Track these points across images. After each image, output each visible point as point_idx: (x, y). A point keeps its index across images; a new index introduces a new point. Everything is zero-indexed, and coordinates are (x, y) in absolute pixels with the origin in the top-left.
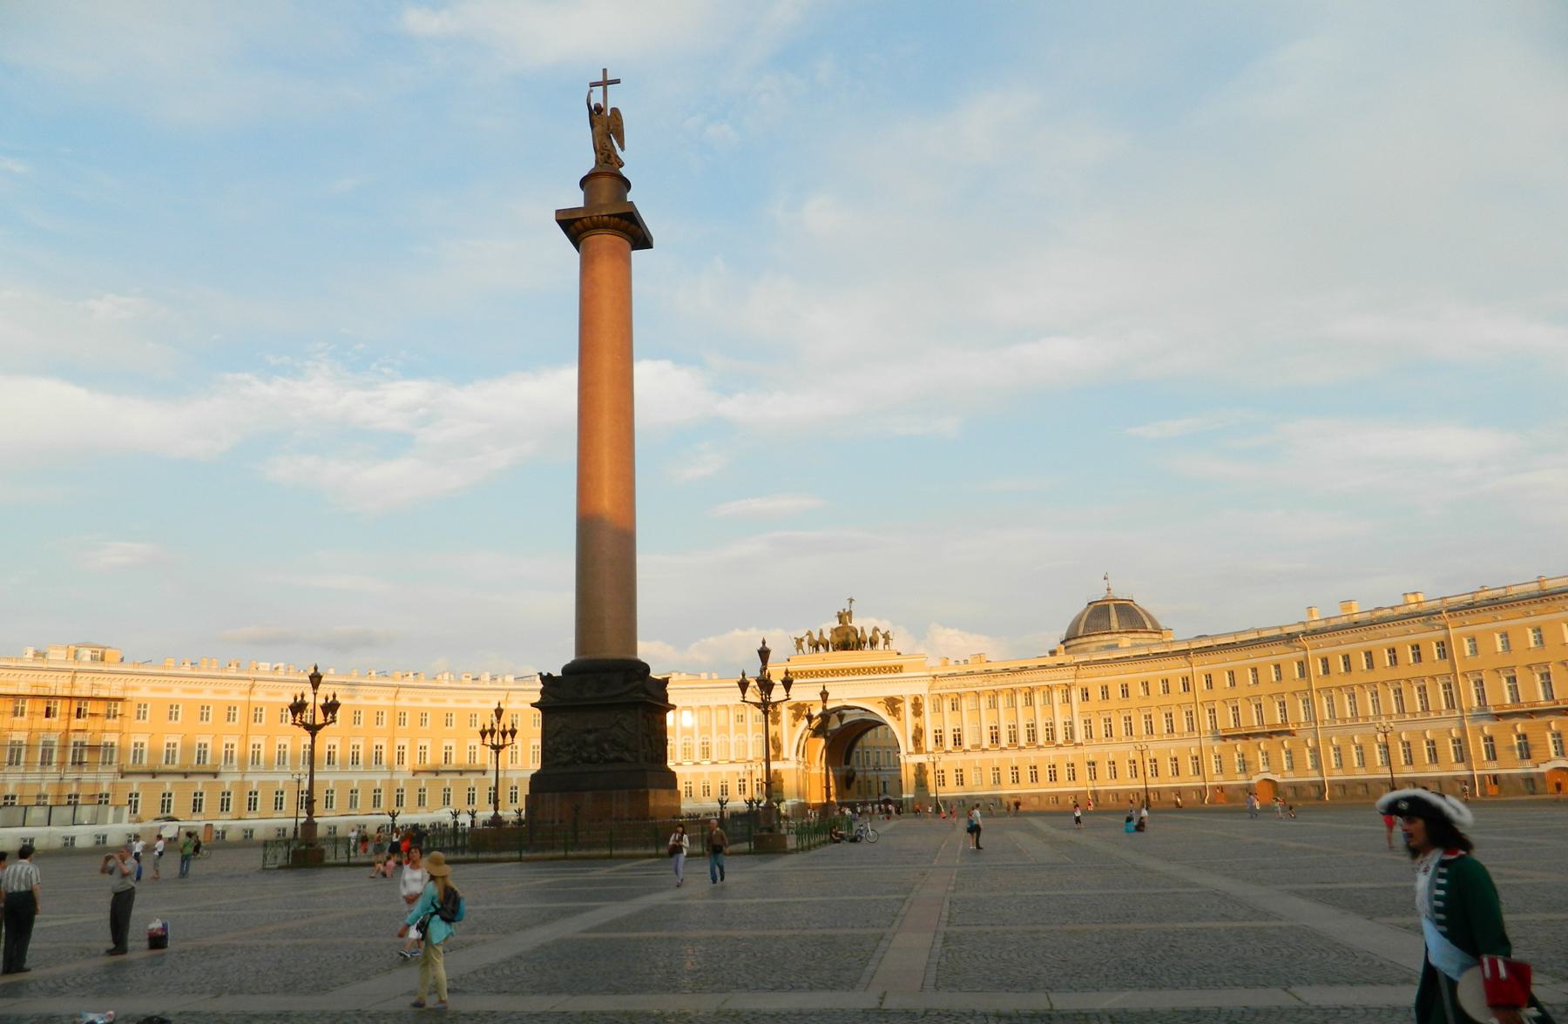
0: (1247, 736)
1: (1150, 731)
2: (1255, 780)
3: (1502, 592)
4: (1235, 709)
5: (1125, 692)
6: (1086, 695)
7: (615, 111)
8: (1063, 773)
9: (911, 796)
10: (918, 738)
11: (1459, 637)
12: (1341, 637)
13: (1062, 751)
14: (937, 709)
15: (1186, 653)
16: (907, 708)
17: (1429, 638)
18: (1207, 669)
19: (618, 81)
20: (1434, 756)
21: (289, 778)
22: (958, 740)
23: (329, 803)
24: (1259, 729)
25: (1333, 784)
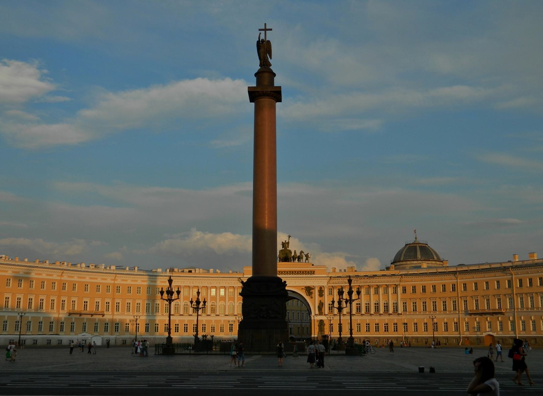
1: (435, 310)
2: (484, 335)
5: (424, 290)
6: (404, 290)
7: (269, 42)
8: (391, 328)
9: (316, 336)
10: (321, 306)
12: (529, 270)
13: (392, 317)
15: (454, 273)
16: (316, 292)
18: (464, 281)
19: (271, 30)
21: (132, 318)
23: (177, 330)
24: (487, 311)
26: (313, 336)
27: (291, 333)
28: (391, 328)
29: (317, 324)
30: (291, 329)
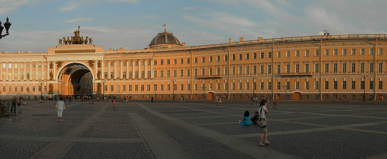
0: (206, 78)
1: (175, 76)
2: (207, 92)
3: (290, 39)
4: (204, 70)
5: (169, 62)
6: (156, 63)
8: (146, 88)
10: (99, 74)
11: (276, 52)
13: (146, 81)
14: (106, 65)
15: (190, 50)
17: (267, 51)
20: (262, 87)
22: (112, 76)
24: (210, 76)
25: (231, 95)
26: (93, 94)
27: (90, 92)
28: (146, 88)
29: (96, 85)
30: (90, 90)
